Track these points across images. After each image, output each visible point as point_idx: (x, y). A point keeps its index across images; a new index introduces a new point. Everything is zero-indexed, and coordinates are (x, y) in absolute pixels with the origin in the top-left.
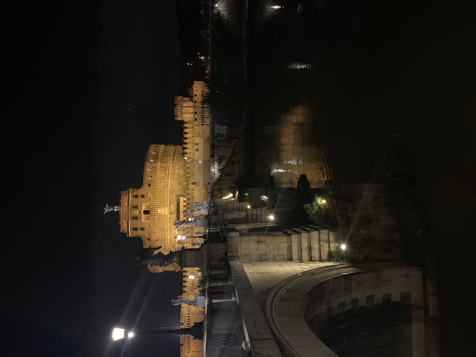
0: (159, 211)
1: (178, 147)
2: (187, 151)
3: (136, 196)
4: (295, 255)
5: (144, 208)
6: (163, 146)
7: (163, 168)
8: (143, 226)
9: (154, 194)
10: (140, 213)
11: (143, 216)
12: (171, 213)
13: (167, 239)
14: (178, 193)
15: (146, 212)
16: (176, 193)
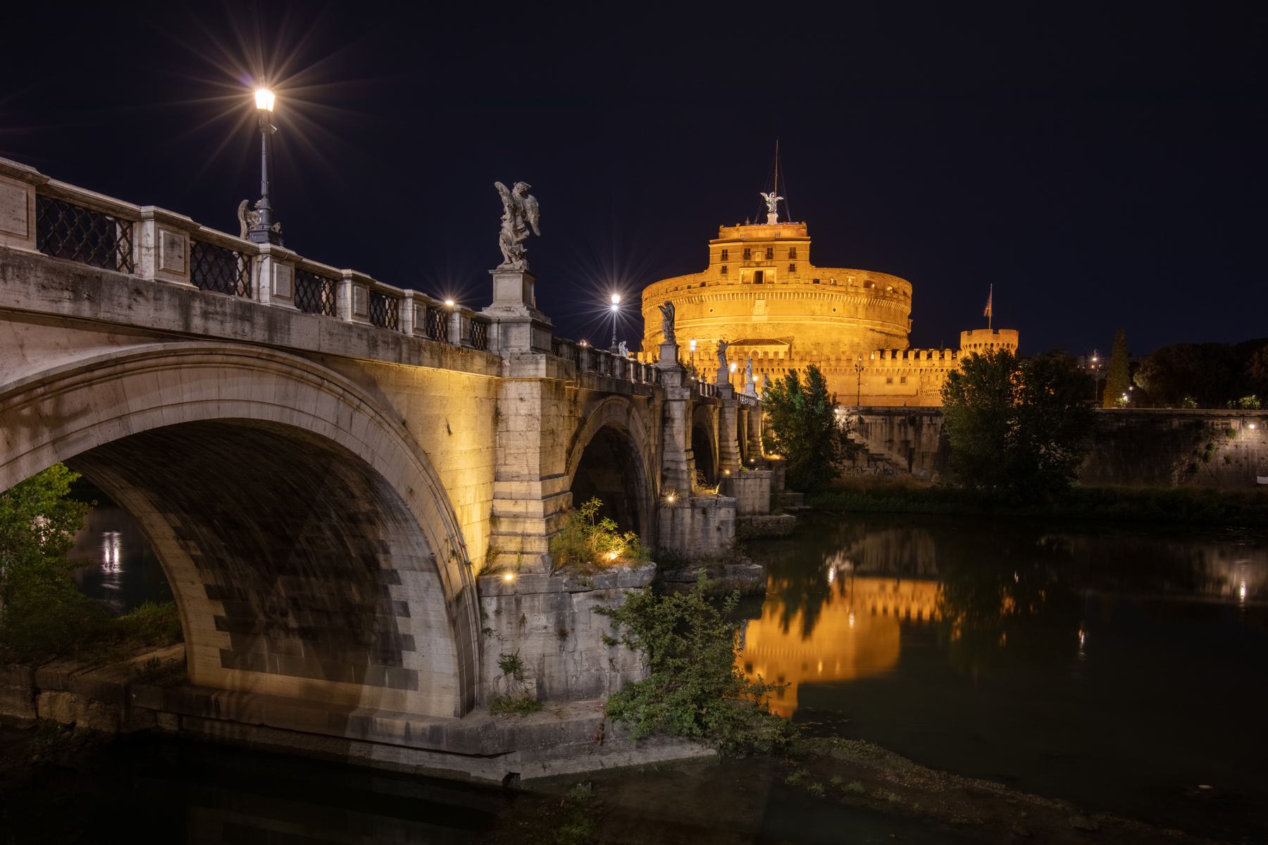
0: (760, 303)
1: (905, 343)
2: (888, 356)
3: (793, 255)
4: (502, 487)
5: (769, 272)
6: (908, 309)
7: (853, 310)
8: (729, 272)
9: (796, 293)
10: (758, 265)
11: (750, 273)
12: (755, 327)
14: (797, 342)
15: (759, 277)
16: (797, 336)
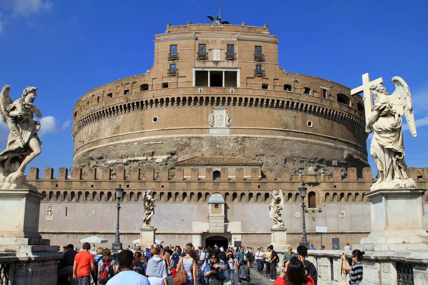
12: (213, 141)
13: (142, 134)
